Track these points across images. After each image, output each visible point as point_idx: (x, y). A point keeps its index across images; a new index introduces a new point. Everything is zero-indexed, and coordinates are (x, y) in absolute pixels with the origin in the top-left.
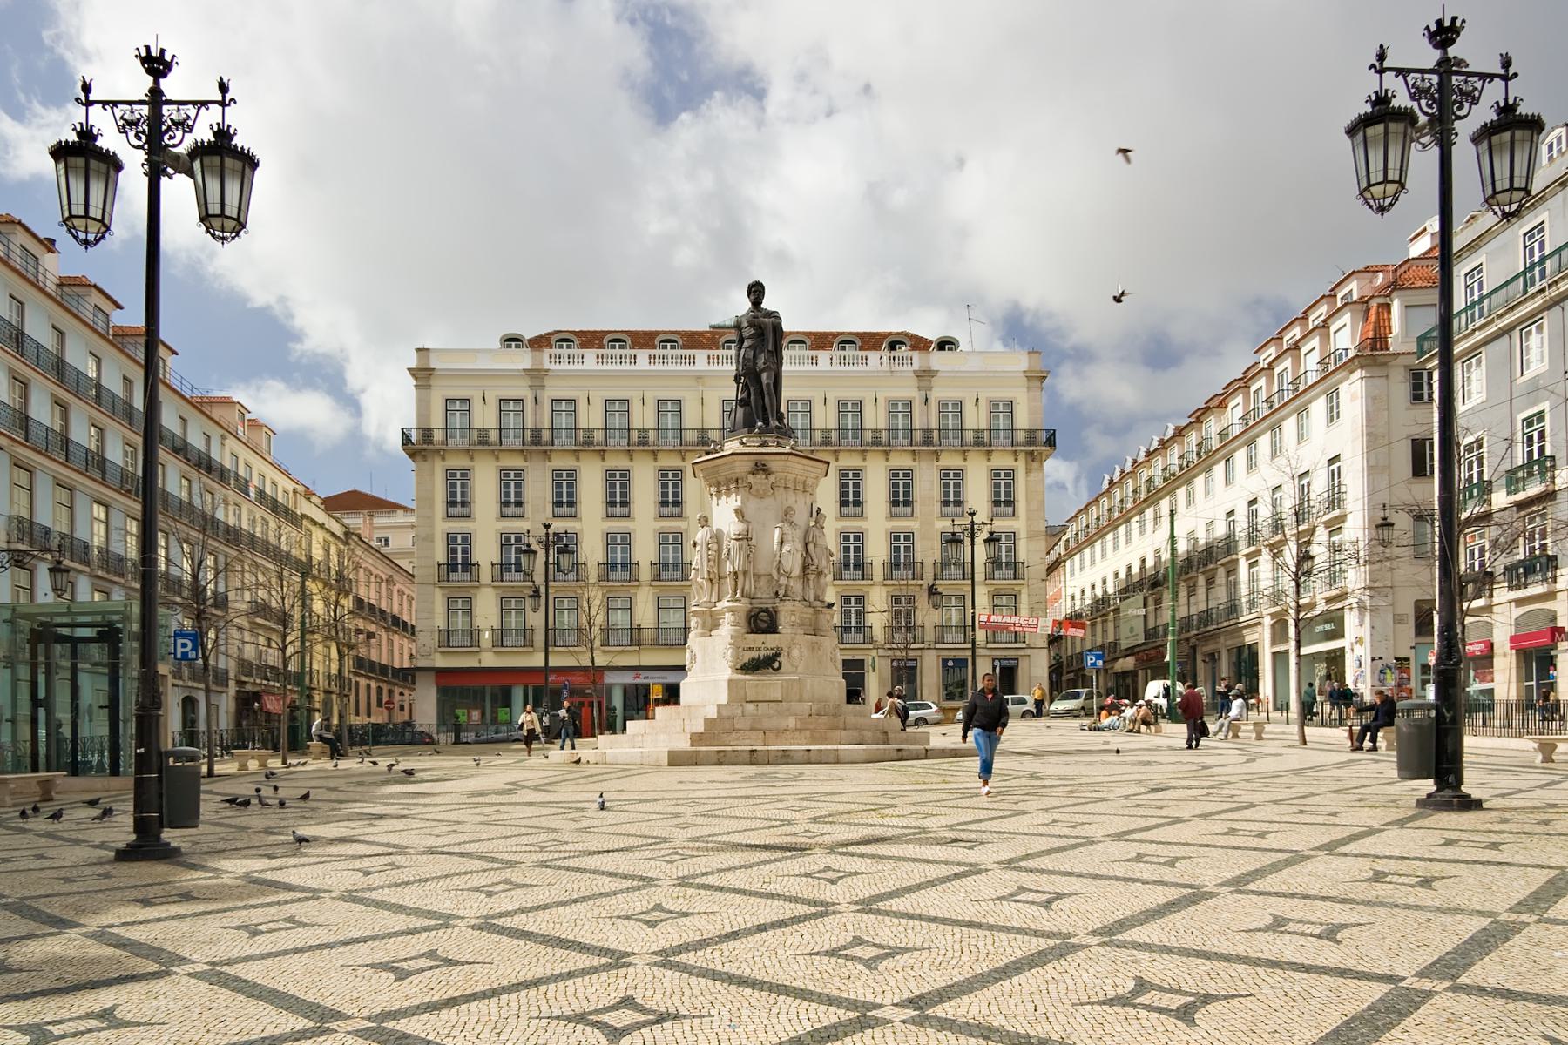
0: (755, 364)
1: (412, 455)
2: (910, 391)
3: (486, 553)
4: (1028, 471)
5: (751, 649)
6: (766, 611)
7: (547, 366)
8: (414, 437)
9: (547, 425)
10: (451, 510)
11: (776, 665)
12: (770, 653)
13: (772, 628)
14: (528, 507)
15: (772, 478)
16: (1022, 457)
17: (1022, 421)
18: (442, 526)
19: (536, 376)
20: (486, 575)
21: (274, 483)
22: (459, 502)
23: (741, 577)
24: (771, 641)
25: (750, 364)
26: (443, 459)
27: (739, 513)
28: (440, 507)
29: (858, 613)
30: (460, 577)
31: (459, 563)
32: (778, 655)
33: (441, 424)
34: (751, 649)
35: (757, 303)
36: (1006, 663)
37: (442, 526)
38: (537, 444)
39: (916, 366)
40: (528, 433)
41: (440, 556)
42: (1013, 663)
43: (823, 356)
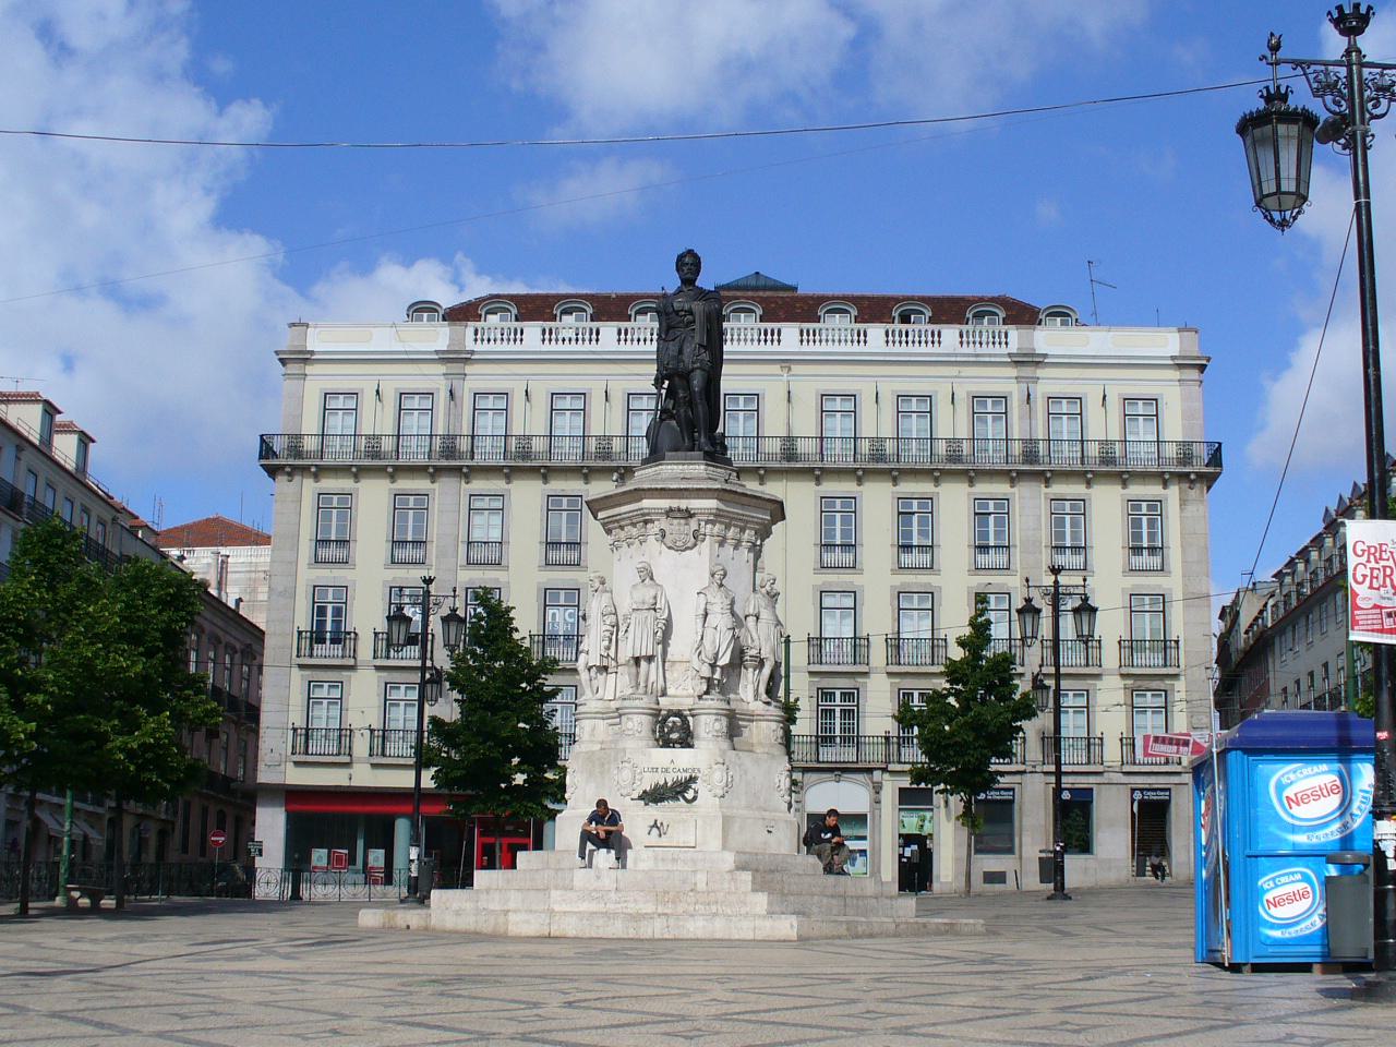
2: (1003, 381)
3: (367, 617)
4: (1183, 502)
6: (678, 714)
7: (470, 345)
9: (466, 430)
11: (690, 795)
12: (684, 776)
13: (686, 741)
14: (432, 549)
15: (693, 524)
17: (1175, 429)
18: (308, 575)
19: (455, 359)
20: (365, 650)
21: (85, 510)
22: (333, 545)
23: (643, 664)
29: (846, 713)
30: (327, 653)
31: (328, 629)
32: (693, 779)
33: (316, 430)
35: (688, 281)
36: (1152, 796)
37: (308, 575)
38: (451, 462)
39: (1013, 347)
40: (437, 442)
41: (303, 621)
42: (1162, 796)
43: (876, 332)
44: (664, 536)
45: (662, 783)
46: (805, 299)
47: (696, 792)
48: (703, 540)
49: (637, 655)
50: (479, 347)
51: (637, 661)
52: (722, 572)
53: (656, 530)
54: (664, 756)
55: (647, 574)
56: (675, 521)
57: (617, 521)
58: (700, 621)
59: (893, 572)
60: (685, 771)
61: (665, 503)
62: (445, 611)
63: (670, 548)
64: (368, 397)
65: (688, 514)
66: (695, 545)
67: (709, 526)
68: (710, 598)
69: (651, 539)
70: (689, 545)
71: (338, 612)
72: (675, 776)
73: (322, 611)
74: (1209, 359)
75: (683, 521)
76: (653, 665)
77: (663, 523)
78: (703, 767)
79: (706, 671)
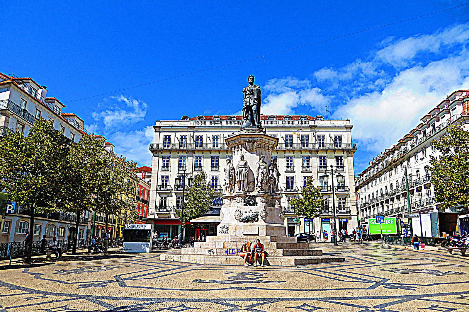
0: (250, 103)
1: (152, 152)
5: (246, 212)
8: (154, 146)
10: (163, 169)
11: (256, 219)
12: (254, 214)
16: (345, 153)
24: (254, 209)
25: (248, 104)
26: (162, 153)
27: (242, 158)
28: (160, 168)
30: (164, 190)
32: (257, 215)
34: (246, 212)
45: (248, 216)
46: (264, 116)
47: (258, 219)
49: (240, 180)
50: (197, 125)
51: (240, 181)
54: (248, 208)
55: (242, 158)
59: (285, 172)
60: (255, 213)
62: (189, 177)
71: (166, 181)
72: (252, 214)
73: (163, 181)
74: (353, 126)
78: (260, 211)
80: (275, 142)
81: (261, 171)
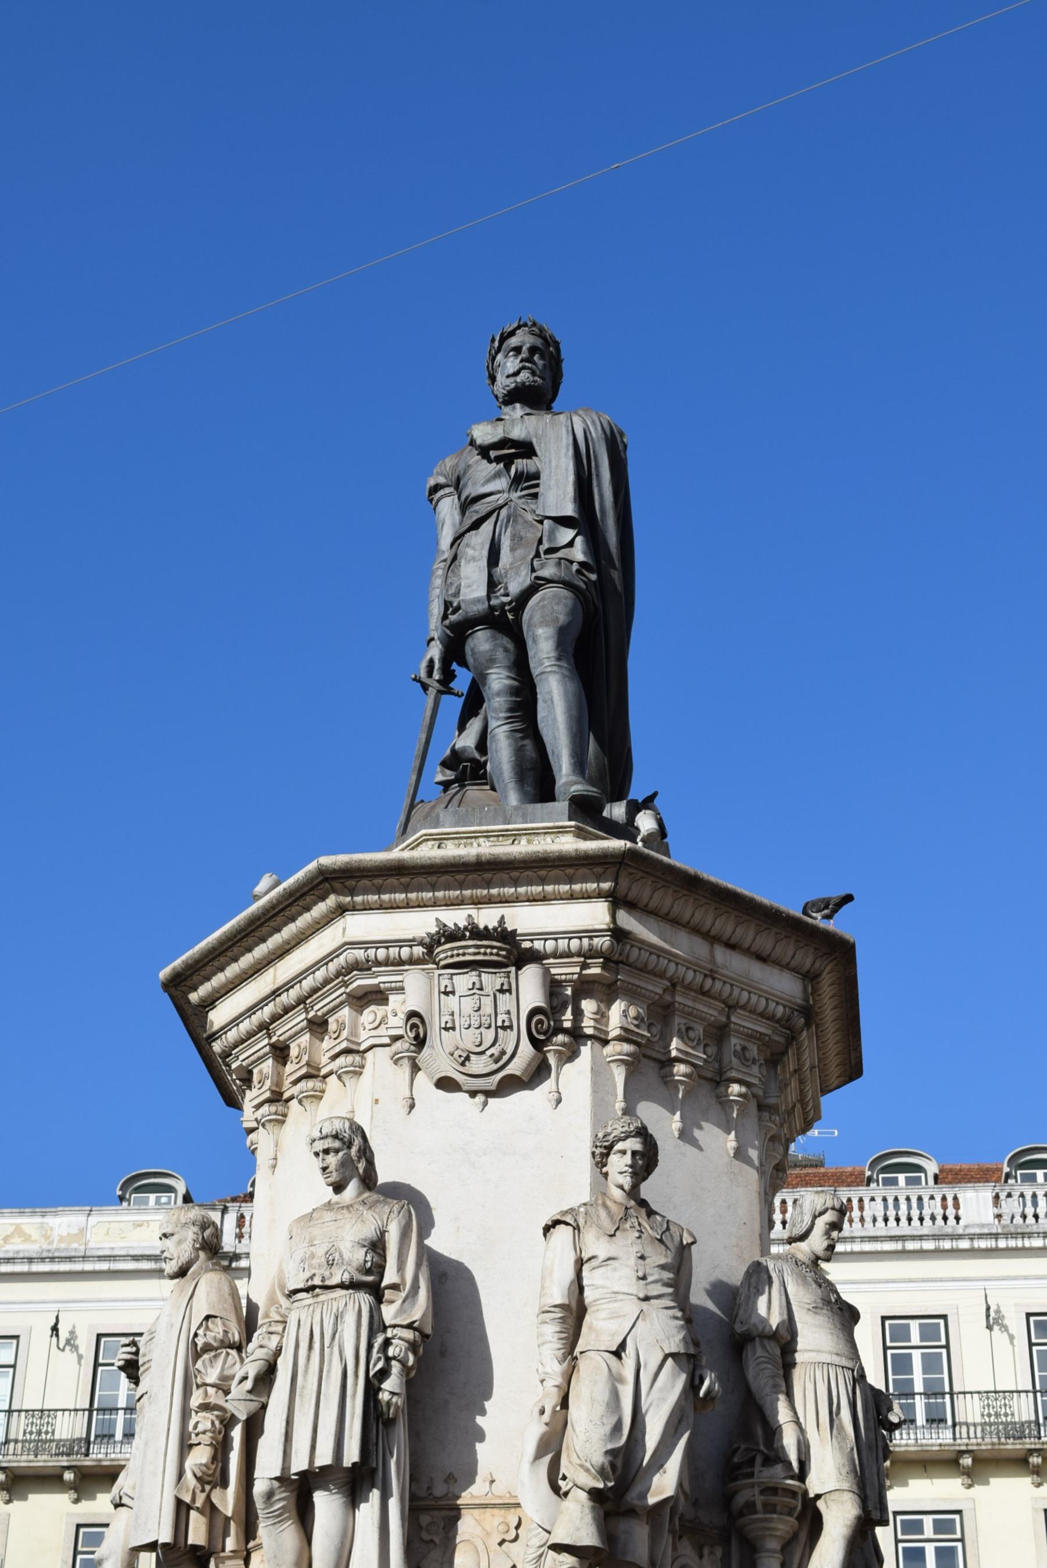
44: (420, 1042)
48: (572, 1055)
49: (299, 1464)
52: (634, 1144)
53: (397, 1024)
56: (464, 981)
57: (264, 1027)
58: (551, 1332)
61: (420, 923)
63: (446, 1084)
64: (38, 1342)
65: (512, 952)
66: (539, 1072)
67: (588, 1006)
68: (595, 1245)
69: (378, 1062)
70: (515, 1068)
75: (491, 981)
76: (368, 1512)
77: (415, 990)
79: (577, 1524)
80: (810, 978)
81: (601, 1328)
